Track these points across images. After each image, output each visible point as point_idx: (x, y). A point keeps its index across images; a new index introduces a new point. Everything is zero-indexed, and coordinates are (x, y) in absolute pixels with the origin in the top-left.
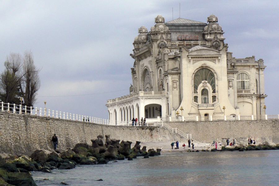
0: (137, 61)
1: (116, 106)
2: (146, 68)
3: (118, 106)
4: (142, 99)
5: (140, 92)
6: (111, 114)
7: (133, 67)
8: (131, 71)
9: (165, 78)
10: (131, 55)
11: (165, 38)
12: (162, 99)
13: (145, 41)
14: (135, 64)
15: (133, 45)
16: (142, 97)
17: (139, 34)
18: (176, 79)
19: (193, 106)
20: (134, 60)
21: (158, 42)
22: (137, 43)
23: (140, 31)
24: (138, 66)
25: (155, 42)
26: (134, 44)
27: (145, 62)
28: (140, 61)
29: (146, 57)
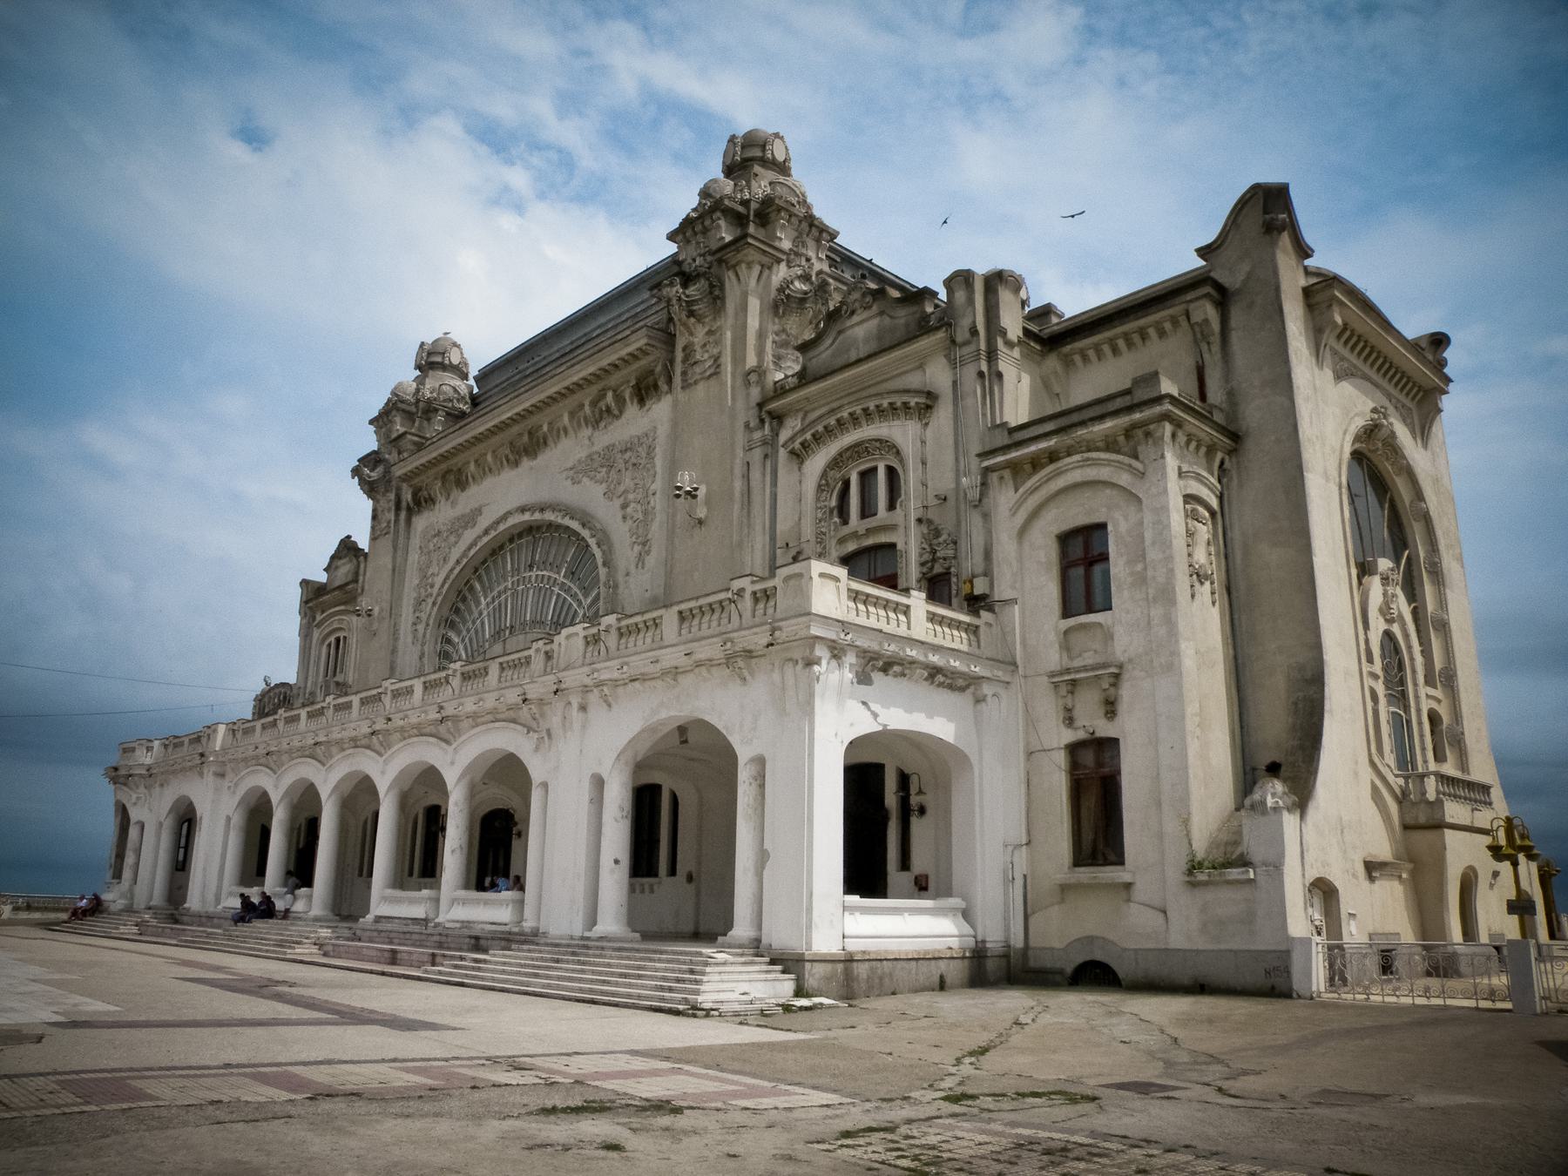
0: (397, 515)
1: (209, 778)
2: (527, 517)
3: (222, 775)
4: (837, 652)
5: (817, 567)
6: (133, 832)
7: (322, 578)
8: (295, 595)
9: (1004, 498)
10: (356, 472)
11: (817, 266)
12: (987, 689)
13: (465, 408)
14: (347, 548)
15: (372, 428)
16: (844, 625)
17: (418, 373)
18: (1205, 493)
19: (1378, 783)
20: (355, 516)
21: (781, 273)
22: (413, 409)
23: (429, 354)
24: (395, 548)
25: (757, 268)
26: (381, 421)
27: (503, 495)
28: (422, 502)
29: (533, 445)
